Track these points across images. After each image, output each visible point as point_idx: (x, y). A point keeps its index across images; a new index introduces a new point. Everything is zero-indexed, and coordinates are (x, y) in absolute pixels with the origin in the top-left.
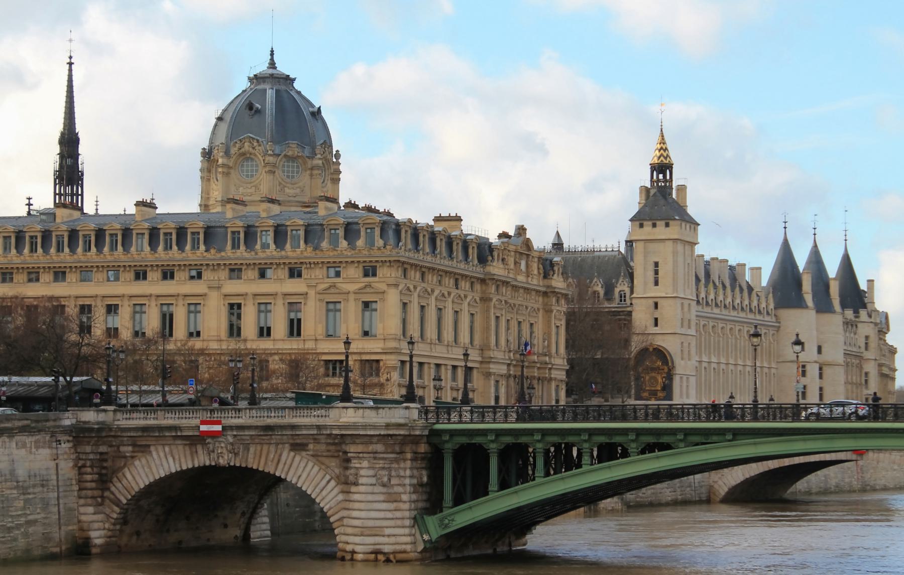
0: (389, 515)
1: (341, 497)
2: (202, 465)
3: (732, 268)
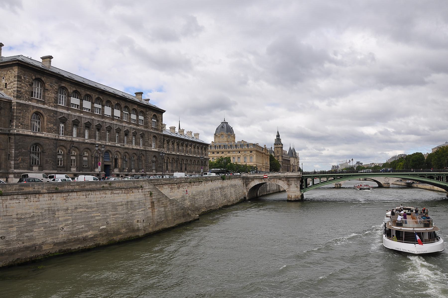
1: (288, 187)
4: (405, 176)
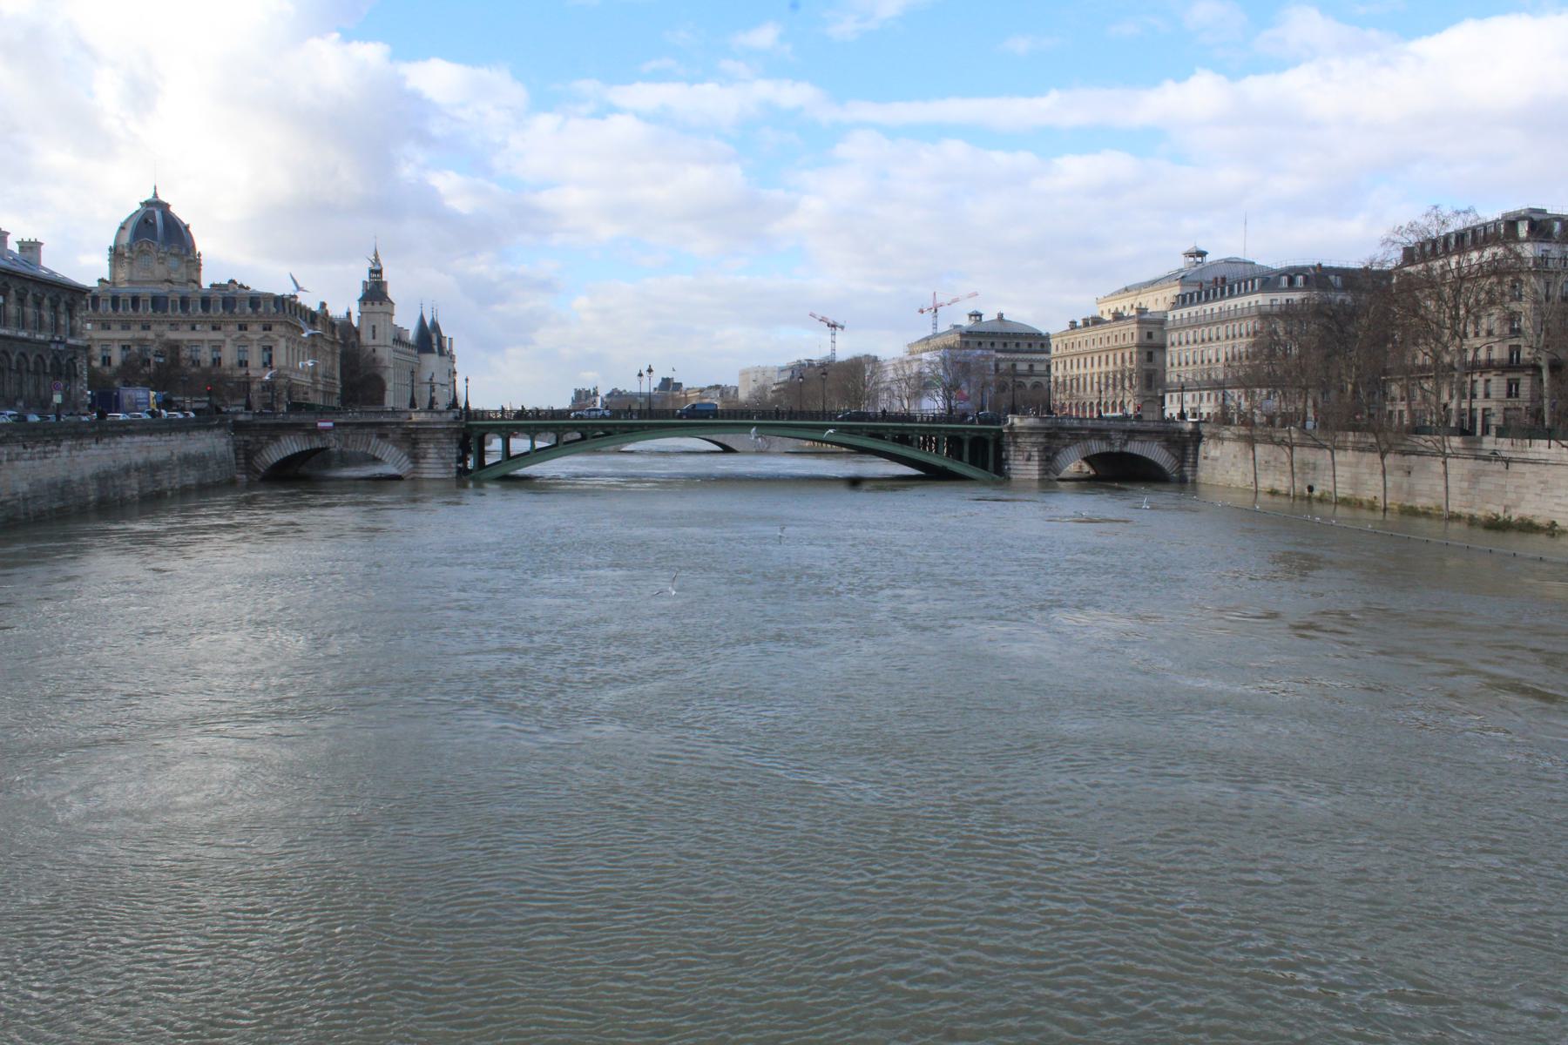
1: (411, 466)
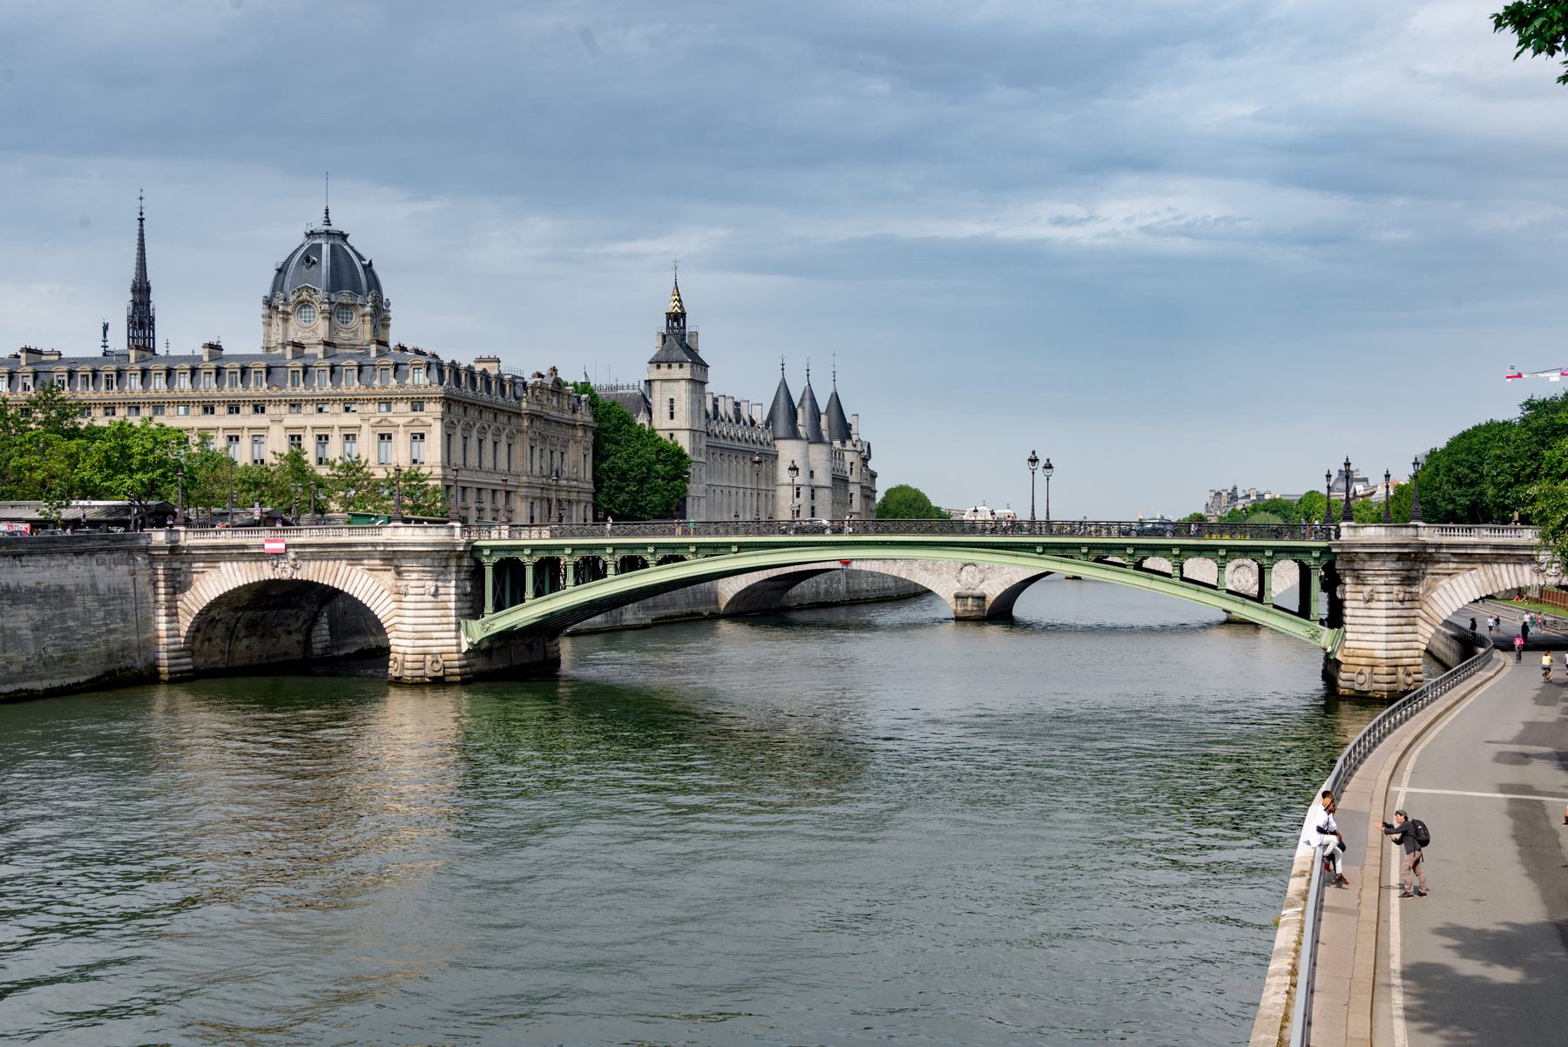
0: (437, 620)
1: (394, 605)
2: (267, 579)
3: (737, 404)
4: (1017, 556)
